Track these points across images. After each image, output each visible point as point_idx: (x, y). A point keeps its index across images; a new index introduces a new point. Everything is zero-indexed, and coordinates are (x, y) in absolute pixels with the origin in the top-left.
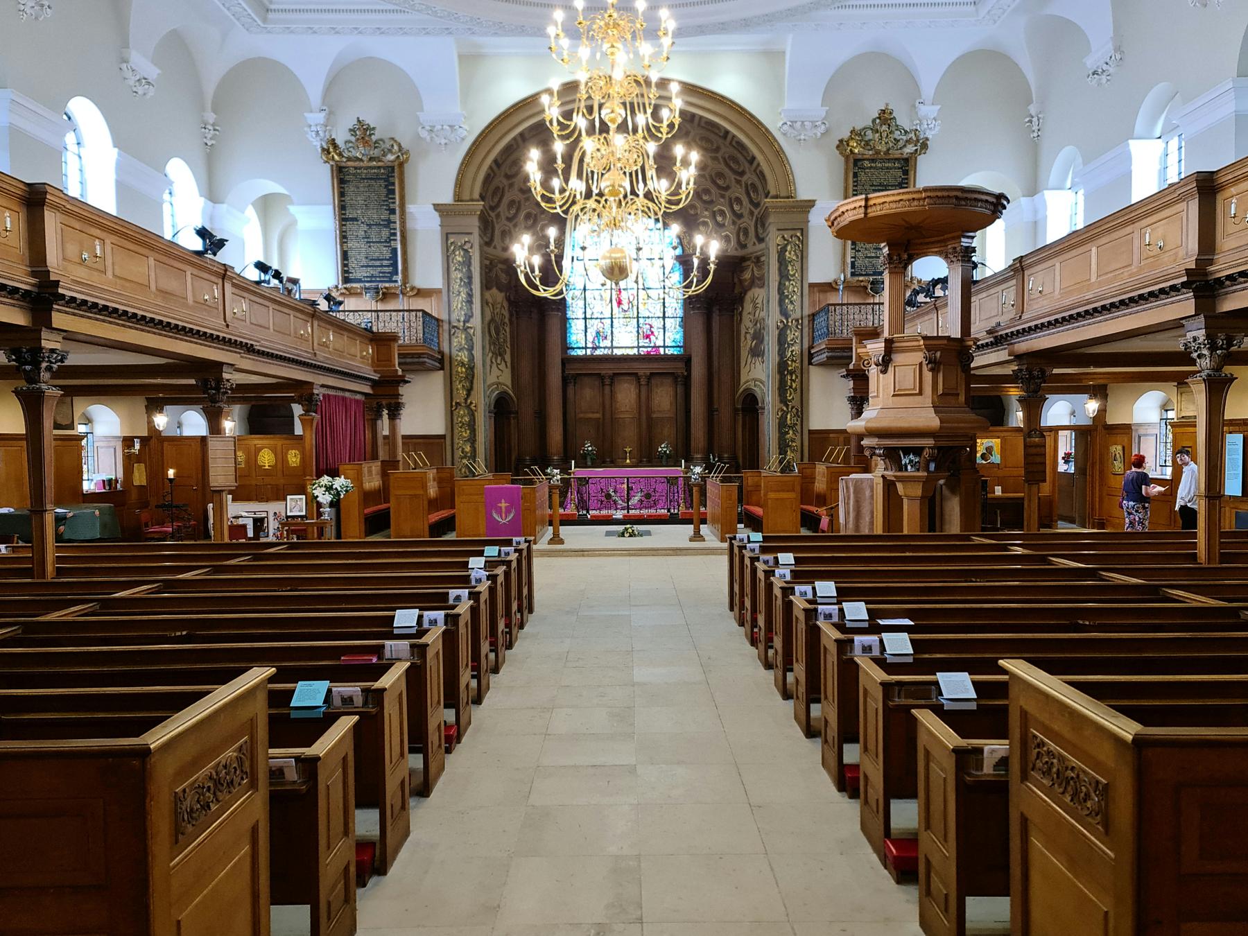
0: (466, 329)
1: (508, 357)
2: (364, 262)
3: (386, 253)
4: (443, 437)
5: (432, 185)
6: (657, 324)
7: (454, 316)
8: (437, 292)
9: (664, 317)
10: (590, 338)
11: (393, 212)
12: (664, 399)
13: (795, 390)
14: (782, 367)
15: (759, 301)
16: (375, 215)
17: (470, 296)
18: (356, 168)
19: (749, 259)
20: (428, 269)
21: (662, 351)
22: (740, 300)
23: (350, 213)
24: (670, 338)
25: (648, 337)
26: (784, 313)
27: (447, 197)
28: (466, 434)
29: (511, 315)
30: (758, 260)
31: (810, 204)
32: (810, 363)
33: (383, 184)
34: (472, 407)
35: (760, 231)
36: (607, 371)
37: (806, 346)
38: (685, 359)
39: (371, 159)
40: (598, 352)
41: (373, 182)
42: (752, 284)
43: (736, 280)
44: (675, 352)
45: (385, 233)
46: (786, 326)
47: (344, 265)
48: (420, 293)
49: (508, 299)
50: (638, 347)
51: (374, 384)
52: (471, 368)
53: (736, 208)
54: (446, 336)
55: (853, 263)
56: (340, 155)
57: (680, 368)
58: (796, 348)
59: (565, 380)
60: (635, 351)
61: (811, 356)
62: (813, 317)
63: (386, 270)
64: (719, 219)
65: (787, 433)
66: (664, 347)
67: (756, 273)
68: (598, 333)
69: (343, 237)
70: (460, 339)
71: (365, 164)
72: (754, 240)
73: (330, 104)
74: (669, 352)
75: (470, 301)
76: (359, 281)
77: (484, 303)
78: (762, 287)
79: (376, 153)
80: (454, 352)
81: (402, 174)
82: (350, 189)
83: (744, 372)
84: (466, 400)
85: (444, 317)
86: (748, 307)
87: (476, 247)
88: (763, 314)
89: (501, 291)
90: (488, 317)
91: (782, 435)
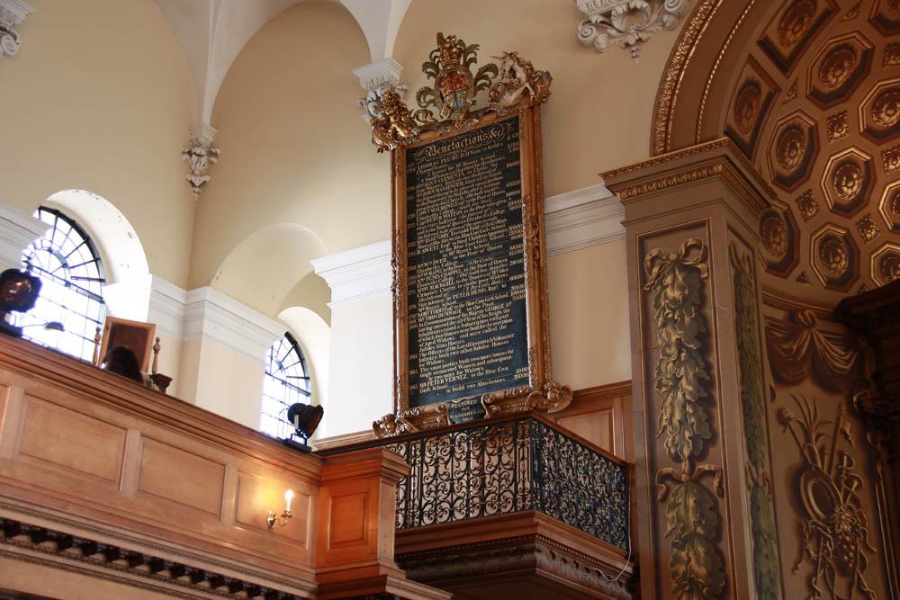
0: (697, 479)
2: (452, 348)
3: (500, 316)
7: (666, 445)
11: (514, 217)
17: (706, 383)
20: (594, 332)
48: (584, 401)
49: (859, 414)
63: (500, 357)
75: (705, 399)
80: (666, 546)
81: (536, 127)
82: (426, 189)
85: (640, 452)
87: (720, 257)
90: (785, 455)
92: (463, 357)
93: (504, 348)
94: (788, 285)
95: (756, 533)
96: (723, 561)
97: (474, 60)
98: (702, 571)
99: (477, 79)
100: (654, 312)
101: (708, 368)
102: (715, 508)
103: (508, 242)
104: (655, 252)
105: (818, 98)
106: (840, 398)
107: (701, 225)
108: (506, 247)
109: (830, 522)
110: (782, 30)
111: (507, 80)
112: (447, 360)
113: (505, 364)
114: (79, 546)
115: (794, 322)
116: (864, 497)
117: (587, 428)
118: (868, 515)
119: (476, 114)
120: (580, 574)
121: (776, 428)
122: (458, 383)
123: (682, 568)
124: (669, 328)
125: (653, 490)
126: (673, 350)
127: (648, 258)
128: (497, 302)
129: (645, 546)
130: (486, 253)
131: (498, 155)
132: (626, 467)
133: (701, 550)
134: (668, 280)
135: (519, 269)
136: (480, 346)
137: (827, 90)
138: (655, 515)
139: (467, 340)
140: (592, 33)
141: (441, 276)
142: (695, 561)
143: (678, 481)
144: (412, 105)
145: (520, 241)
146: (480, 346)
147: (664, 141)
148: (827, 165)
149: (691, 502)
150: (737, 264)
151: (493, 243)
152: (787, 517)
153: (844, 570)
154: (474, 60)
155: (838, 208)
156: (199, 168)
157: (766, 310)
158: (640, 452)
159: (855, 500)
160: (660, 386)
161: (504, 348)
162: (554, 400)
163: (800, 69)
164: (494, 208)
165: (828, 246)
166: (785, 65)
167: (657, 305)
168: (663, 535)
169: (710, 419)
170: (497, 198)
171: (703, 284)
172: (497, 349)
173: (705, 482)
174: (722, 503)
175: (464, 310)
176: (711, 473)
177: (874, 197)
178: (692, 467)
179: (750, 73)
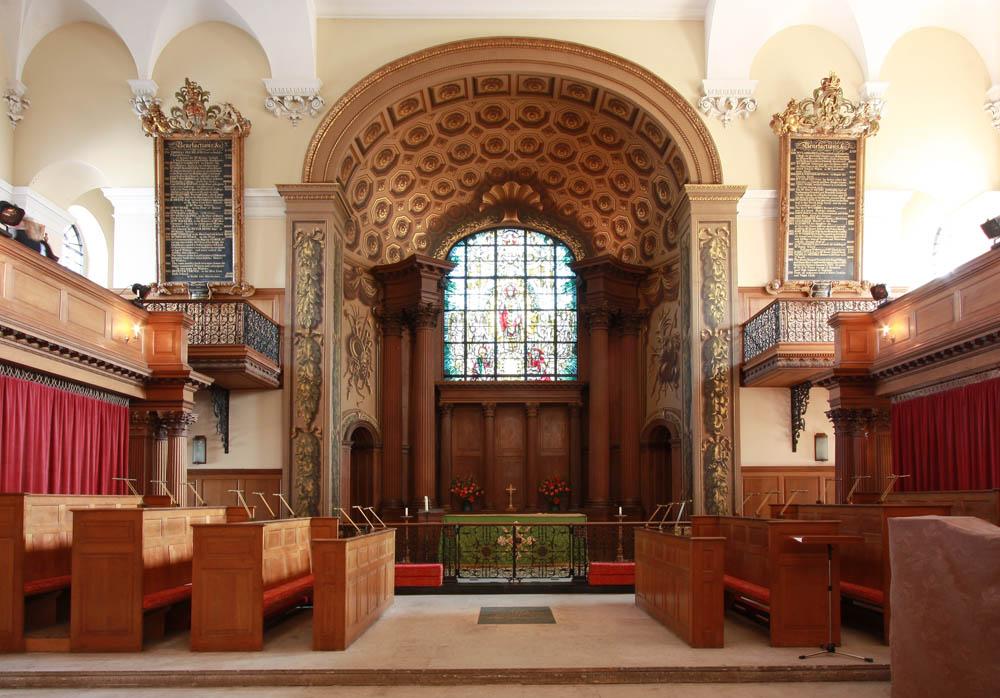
0: (312, 337)
1: (371, 382)
2: (191, 256)
4: (279, 472)
5: (276, 161)
6: (548, 349)
7: (299, 321)
8: (280, 292)
9: (555, 342)
12: (553, 435)
13: (724, 416)
14: (708, 386)
15: (671, 316)
16: (204, 199)
17: (319, 296)
18: (184, 142)
19: (656, 271)
21: (553, 379)
22: (646, 318)
23: (175, 196)
24: (562, 365)
25: (536, 364)
26: (709, 321)
27: (296, 178)
28: (308, 469)
29: (378, 333)
30: (668, 270)
32: (743, 385)
33: (216, 160)
34: (317, 434)
35: (671, 235)
37: (737, 361)
38: (581, 384)
39: (203, 131)
40: (480, 379)
41: (205, 159)
42: (662, 296)
43: (640, 296)
45: (217, 220)
46: (712, 338)
47: (168, 259)
48: (259, 293)
49: (375, 315)
51: (146, 383)
52: (317, 384)
53: (640, 215)
54: (287, 346)
55: (791, 264)
56: (166, 125)
57: (573, 398)
58: (725, 365)
59: (439, 412)
60: (523, 379)
61: (743, 375)
62: (744, 325)
64: (619, 230)
65: (715, 470)
66: (556, 375)
67: (666, 285)
68: (480, 360)
69: (166, 225)
70: (305, 349)
71: (195, 137)
72: (664, 248)
73: (160, 76)
74: (564, 379)
75: (318, 302)
76: (185, 278)
78: (674, 298)
79: (211, 124)
80: (296, 363)
83: (650, 401)
86: (657, 324)
88: (675, 331)
89: (366, 304)
90: (346, 330)
91: (709, 473)
92: (197, 261)
93: (220, 261)
94: (353, 255)
95: (334, 362)
96: (321, 372)
98: (311, 375)
99: (208, 112)
100: (298, 259)
101: (321, 289)
102: (319, 350)
103: (223, 207)
104: (300, 230)
105: (377, 172)
106: (368, 308)
107: (323, 222)
108: (222, 209)
109: (359, 359)
110: (366, 135)
111: (225, 117)
113: (220, 269)
114: (39, 342)
115: (354, 273)
116: (373, 349)
117: (261, 306)
118: (373, 357)
119: (207, 131)
120: (261, 373)
121: (344, 318)
122: (194, 273)
123: (302, 373)
124: (304, 268)
125: (292, 339)
126: (305, 278)
127: (297, 232)
128: (216, 237)
129: (287, 363)
130: (211, 210)
131: (219, 158)
132: (279, 328)
133: (311, 366)
134: (306, 245)
135: (230, 222)
136: (207, 257)
137: (379, 168)
138: (292, 350)
139: (200, 253)
140: (273, 106)
141: (184, 217)
142: (308, 371)
143: (304, 337)
144: (168, 114)
145: (231, 208)
146: (207, 257)
147: (309, 178)
148: (374, 202)
149: (309, 346)
150: (336, 243)
151: (215, 205)
152: (344, 354)
153: (362, 377)
154: (206, 100)
155: (377, 223)
156: (15, 110)
157: (345, 266)
158: (287, 322)
159: (369, 350)
161: (220, 261)
162: (244, 292)
163: (370, 156)
164: (216, 187)
165: (371, 240)
166: (364, 152)
167: (299, 256)
168: (295, 359)
169: (320, 312)
170: (219, 181)
171: (321, 250)
172: (216, 261)
173: (315, 339)
174: (323, 348)
175: (198, 237)
177: (391, 223)
178: (311, 331)
179: (349, 152)
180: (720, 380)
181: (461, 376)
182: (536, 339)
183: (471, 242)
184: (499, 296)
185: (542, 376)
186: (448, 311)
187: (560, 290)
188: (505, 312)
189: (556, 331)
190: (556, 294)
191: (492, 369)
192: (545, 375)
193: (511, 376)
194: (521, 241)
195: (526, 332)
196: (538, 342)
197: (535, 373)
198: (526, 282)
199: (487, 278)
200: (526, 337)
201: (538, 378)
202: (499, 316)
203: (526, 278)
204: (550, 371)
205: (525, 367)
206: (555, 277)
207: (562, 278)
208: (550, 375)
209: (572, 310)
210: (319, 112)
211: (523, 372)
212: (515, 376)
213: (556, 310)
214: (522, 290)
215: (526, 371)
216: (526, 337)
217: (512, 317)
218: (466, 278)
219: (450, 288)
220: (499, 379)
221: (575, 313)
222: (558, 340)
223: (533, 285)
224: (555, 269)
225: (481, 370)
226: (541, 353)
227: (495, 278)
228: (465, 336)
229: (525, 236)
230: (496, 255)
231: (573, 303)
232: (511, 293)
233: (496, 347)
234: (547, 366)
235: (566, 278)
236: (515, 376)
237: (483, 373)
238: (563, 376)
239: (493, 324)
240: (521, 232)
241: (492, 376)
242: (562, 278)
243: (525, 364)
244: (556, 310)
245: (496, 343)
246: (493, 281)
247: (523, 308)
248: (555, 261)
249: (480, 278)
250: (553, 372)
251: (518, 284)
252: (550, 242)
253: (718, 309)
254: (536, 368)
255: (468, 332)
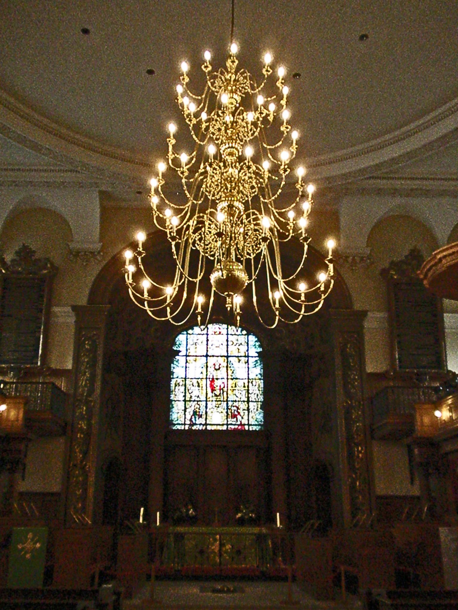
9: (248, 402)
10: (188, 417)
17: (93, 376)
21: (246, 427)
24: (253, 418)
25: (234, 416)
26: (348, 395)
31: (363, 314)
36: (203, 441)
40: (194, 428)
44: (257, 428)
50: (227, 425)
60: (225, 428)
66: (249, 425)
68: (195, 413)
74: (254, 428)
75: (92, 380)
77: (104, 382)
84: (82, 462)
85: (72, 392)
97: (34, 256)
112: (10, 351)
126: (85, 364)
149: (85, 408)
158: (72, 392)
160: (80, 373)
176: (91, 401)
180: (357, 434)
181: (182, 424)
182: (235, 398)
183: (190, 331)
184: (208, 368)
185: (238, 425)
186: (173, 378)
187: (251, 365)
188: (213, 380)
189: (248, 393)
190: (248, 368)
191: (204, 419)
192: (241, 424)
193: (217, 425)
194: (224, 332)
195: (227, 394)
196: (236, 401)
197: (234, 423)
198: (227, 359)
199: (201, 356)
200: (227, 397)
201: (236, 427)
202: (209, 383)
203: (227, 357)
204: (245, 421)
205: (227, 419)
206: (248, 356)
207: (252, 357)
208: (245, 425)
209: (260, 379)
210: (100, 261)
211: (225, 422)
212: (219, 425)
213: (248, 379)
214: (225, 364)
215: (227, 421)
216: (227, 397)
217: (217, 383)
218: (187, 356)
219: (175, 362)
220: (209, 428)
221: (262, 381)
222: (250, 400)
223: (233, 362)
224: (248, 350)
225: (196, 421)
226: (238, 408)
227: (207, 356)
228: (185, 396)
229: (227, 329)
230: (208, 340)
231: (260, 374)
232: (217, 367)
233: (207, 404)
234: (242, 418)
235: (255, 357)
236: (219, 425)
237: (197, 422)
238: (254, 425)
239: (204, 388)
240: (225, 326)
241: (203, 425)
242: (252, 357)
243: (227, 416)
244: (248, 379)
245: (206, 401)
246: (205, 358)
247: (226, 377)
248: (248, 345)
249: (196, 356)
250: (247, 423)
251: (222, 361)
252: (244, 332)
253: (354, 387)
254: (235, 419)
255: (187, 394)
